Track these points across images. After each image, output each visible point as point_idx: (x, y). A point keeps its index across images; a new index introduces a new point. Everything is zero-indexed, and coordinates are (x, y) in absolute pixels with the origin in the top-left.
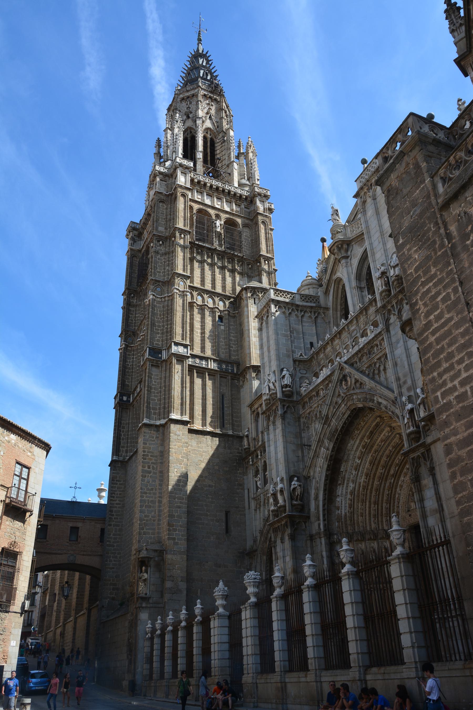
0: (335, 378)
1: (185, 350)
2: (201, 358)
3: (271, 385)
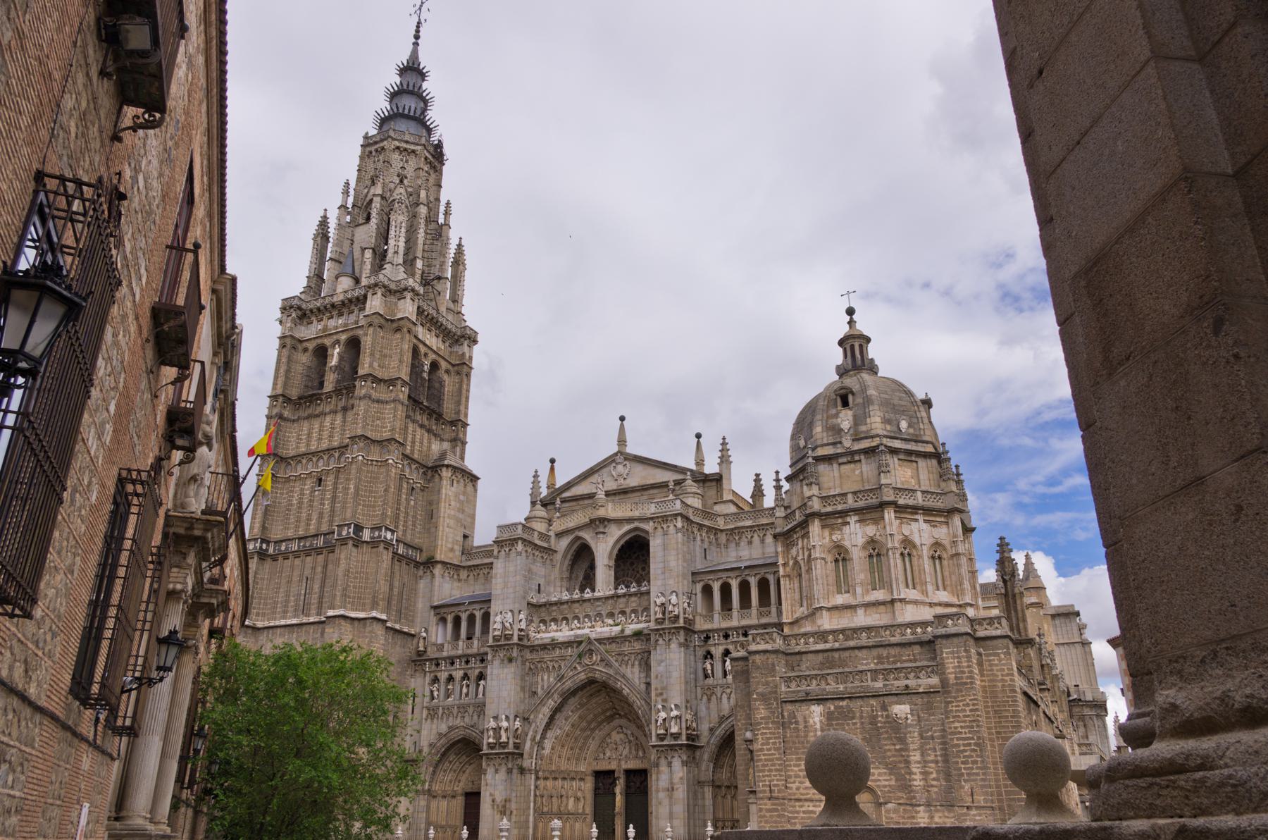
3: (508, 625)
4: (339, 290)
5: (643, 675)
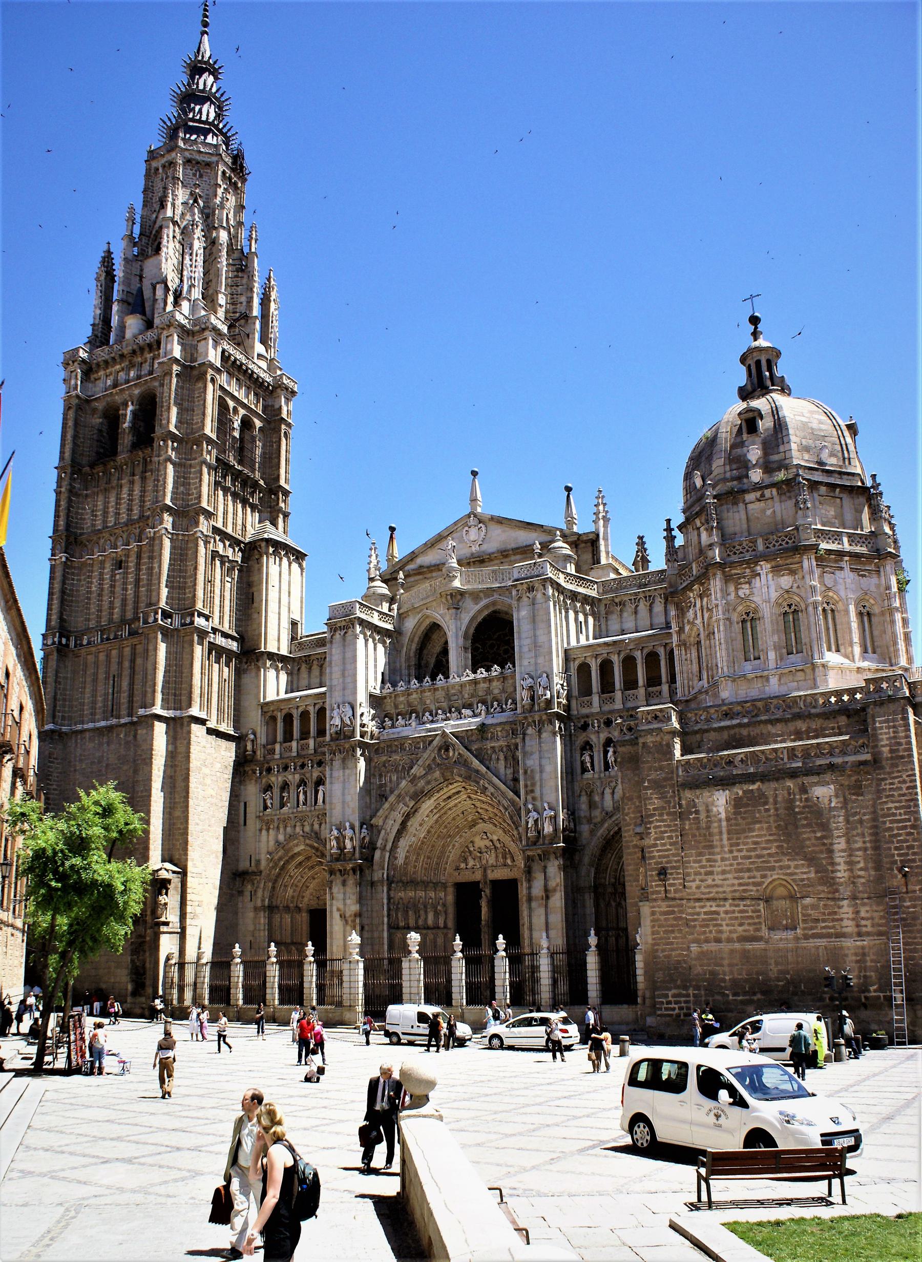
4: (129, 334)
5: (510, 771)
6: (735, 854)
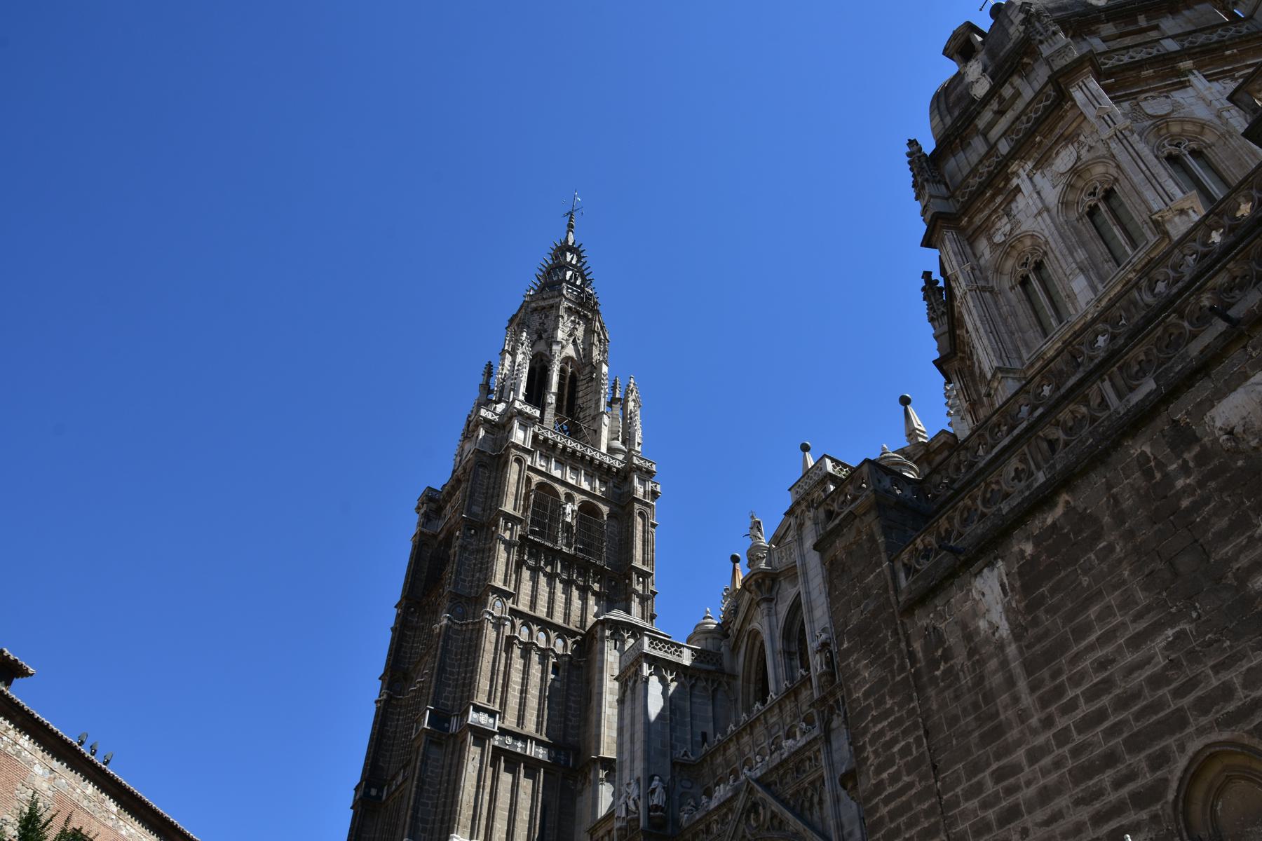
0: (739, 804)
1: (491, 721)
2: (517, 736)
3: (631, 803)
6: (1061, 723)
